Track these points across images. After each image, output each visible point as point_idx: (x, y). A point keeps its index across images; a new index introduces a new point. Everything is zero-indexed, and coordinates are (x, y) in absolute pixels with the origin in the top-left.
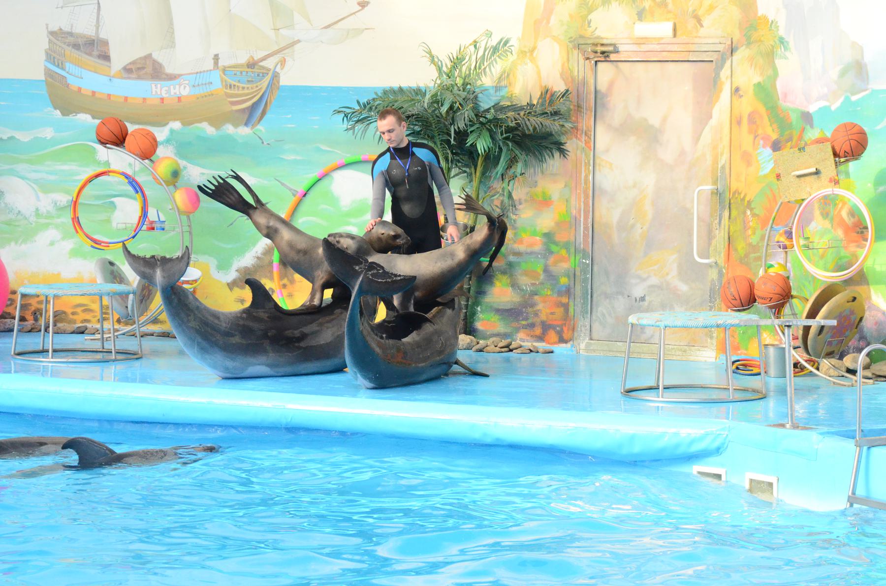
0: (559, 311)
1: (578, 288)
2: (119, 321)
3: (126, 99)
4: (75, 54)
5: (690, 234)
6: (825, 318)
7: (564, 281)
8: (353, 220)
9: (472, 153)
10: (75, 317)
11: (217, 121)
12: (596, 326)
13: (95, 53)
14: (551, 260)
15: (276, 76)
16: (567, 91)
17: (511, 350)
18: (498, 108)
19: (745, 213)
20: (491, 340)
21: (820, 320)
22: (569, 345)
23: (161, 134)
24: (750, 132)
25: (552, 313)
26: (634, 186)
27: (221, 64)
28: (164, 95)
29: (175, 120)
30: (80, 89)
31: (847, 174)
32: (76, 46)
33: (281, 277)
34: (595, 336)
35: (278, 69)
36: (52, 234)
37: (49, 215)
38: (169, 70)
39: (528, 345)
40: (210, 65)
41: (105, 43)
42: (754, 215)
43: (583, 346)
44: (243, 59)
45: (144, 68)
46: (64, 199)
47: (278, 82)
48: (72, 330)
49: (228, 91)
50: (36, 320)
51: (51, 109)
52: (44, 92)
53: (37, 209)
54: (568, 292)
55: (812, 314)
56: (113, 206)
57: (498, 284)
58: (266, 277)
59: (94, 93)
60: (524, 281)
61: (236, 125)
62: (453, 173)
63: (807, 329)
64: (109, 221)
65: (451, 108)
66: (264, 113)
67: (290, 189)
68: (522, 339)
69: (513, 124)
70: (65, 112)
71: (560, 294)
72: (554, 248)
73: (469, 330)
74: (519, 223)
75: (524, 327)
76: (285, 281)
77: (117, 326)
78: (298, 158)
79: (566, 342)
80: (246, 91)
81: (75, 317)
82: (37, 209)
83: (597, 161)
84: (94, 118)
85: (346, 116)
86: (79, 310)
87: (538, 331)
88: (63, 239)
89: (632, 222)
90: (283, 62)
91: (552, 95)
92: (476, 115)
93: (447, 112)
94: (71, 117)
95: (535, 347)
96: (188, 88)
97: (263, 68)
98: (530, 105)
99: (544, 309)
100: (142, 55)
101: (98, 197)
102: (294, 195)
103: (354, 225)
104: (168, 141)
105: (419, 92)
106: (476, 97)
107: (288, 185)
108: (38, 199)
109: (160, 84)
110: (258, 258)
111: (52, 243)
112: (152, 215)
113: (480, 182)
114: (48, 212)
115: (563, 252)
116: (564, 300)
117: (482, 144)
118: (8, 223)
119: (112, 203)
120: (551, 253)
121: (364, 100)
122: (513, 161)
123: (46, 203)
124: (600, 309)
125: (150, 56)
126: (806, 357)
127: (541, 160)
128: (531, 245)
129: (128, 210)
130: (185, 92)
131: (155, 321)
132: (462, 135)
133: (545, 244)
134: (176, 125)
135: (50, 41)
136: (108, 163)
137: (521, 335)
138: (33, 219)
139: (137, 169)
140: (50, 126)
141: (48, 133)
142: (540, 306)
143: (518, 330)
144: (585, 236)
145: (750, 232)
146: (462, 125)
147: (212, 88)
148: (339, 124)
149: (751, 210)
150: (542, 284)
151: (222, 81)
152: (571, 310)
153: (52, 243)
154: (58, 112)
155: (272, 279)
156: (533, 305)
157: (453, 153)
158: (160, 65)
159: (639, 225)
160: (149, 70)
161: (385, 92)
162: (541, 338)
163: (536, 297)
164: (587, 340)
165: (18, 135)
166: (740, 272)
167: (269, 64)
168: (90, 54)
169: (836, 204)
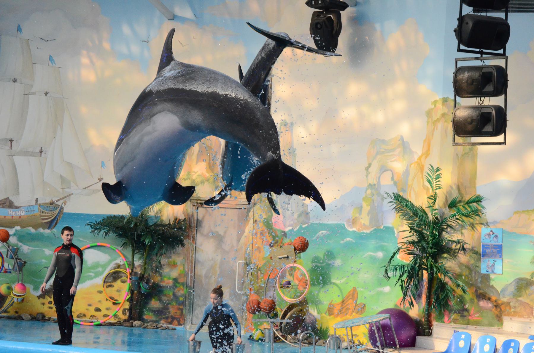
0: (179, 312)
1: (187, 303)
5: (235, 281)
6: (290, 319)
7: (181, 299)
8: (92, 271)
9: (144, 245)
11: (36, 227)
12: (194, 318)
14: (176, 290)
15: (62, 208)
16: (185, 219)
17: (158, 328)
18: (156, 225)
19: (258, 273)
20: (150, 323)
21: (286, 321)
22: (182, 326)
23: (11, 232)
24: (260, 238)
25: (176, 313)
26: (212, 259)
27: (38, 202)
28: (14, 215)
31: (300, 258)
34: (194, 322)
35: (63, 206)
38: (16, 204)
39: (165, 326)
40: (34, 203)
42: (261, 273)
43: (188, 327)
44: (48, 201)
49: (41, 214)
54: (183, 303)
55: (284, 317)
57: (153, 300)
60: (164, 299)
61: (44, 229)
62: (136, 252)
63: (281, 323)
65: (136, 225)
66: (56, 224)
68: (163, 323)
69: (161, 232)
71: (179, 304)
72: (178, 285)
73: (140, 318)
74: (163, 274)
75: (164, 318)
79: (181, 325)
83: (197, 249)
85: (91, 226)
87: (170, 320)
89: (210, 275)
91: (180, 220)
92: (147, 228)
93: (134, 226)
95: (168, 327)
96: (24, 212)
97: (57, 205)
98: (169, 224)
99: (173, 310)
100: (5, 197)
103: (93, 272)
104: (14, 235)
105: (123, 217)
106: (147, 220)
112: (6, 266)
113: (147, 256)
115: (181, 287)
116: (181, 307)
117: (147, 242)
120: (176, 287)
121: (98, 221)
122: (161, 248)
124: (196, 311)
125: (8, 198)
126: (282, 334)
127: (174, 248)
128: (168, 283)
131: (5, 311)
132: (139, 236)
133: (174, 283)
134: (18, 228)
137: (162, 322)
142: (171, 310)
143: (161, 319)
144: (191, 280)
145: (259, 281)
146: (139, 232)
147: (35, 213)
148: (88, 229)
149: (261, 271)
150: (172, 300)
152: (184, 311)
156: (168, 309)
157: (136, 244)
158: (13, 202)
159: (213, 276)
160: (8, 204)
161: (108, 217)
162: (171, 323)
163: (169, 306)
164: (190, 324)
166: (254, 297)
167: (59, 203)
169: (295, 270)
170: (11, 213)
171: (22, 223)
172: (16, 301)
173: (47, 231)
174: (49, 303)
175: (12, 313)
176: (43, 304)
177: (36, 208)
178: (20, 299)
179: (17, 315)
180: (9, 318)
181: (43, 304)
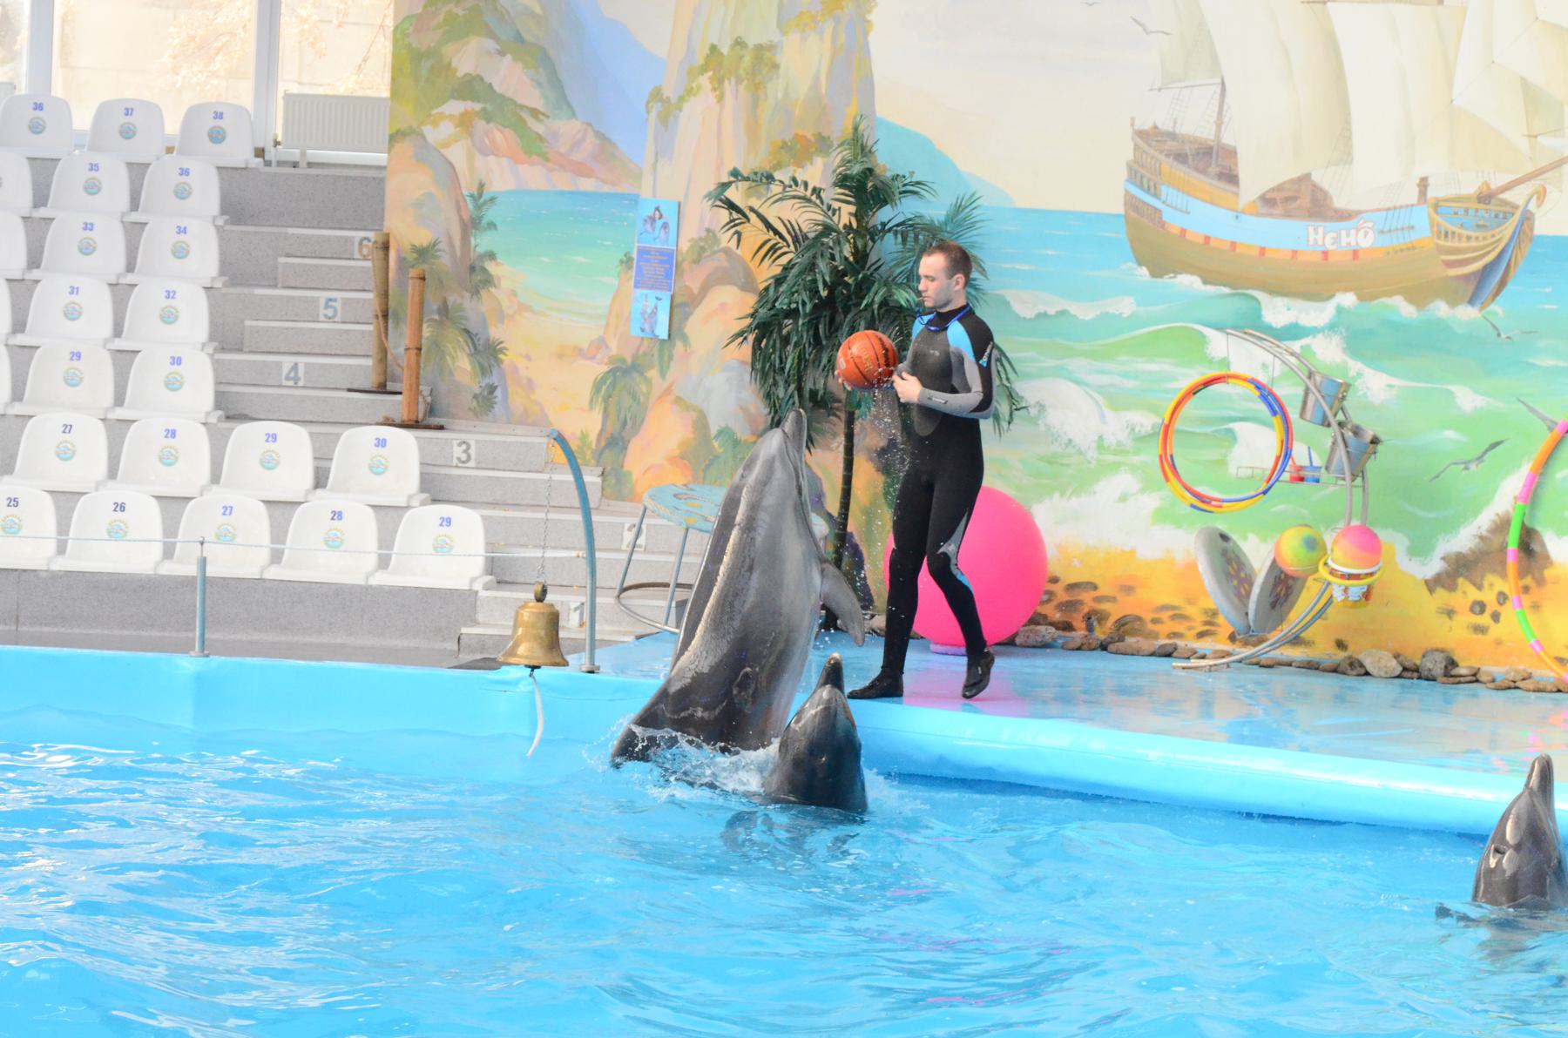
2: (1232, 638)
3: (1263, 250)
4: (1180, 170)
10: (1157, 628)
11: (1419, 295)
13: (1213, 169)
15: (1527, 218)
28: (1329, 246)
29: (1346, 290)
30: (1183, 231)
32: (1181, 157)
33: (1522, 573)
35: (1532, 207)
36: (1125, 481)
37: (1120, 450)
38: (1339, 202)
40: (1412, 195)
41: (1231, 153)
44: (1470, 187)
45: (1294, 198)
46: (1148, 421)
47: (1532, 229)
48: (1152, 649)
49: (1442, 242)
50: (1090, 629)
51: (1132, 264)
52: (1121, 234)
53: (1101, 438)
56: (1231, 436)
58: (1494, 571)
59: (1207, 239)
61: (1453, 304)
64: (1222, 463)
66: (1503, 283)
67: (1544, 419)
70: (1157, 272)
76: (1528, 580)
77: (1228, 647)
78: (1561, 364)
80: (1473, 244)
81: (1157, 628)
82: (1101, 438)
84: (1205, 282)
86: (1165, 615)
88: (1143, 491)
90: (1541, 195)
94: (1166, 279)
96: (1371, 236)
97: (1505, 203)
101: (1206, 421)
102: (1550, 429)
104: (1332, 327)
107: (1541, 411)
108: (1103, 417)
109: (1322, 226)
110: (1481, 538)
111: (1123, 498)
112: (1300, 454)
114: (1119, 443)
118: (1051, 460)
119: (1230, 431)
123: (1116, 427)
129: (1257, 445)
130: (1366, 241)
131: (1296, 641)
134: (1348, 299)
135: (1136, 148)
136: (1225, 362)
138: (1092, 454)
139: (1277, 374)
140: (1128, 293)
141: (1126, 306)
151: (1432, 227)
153: (1123, 498)
154: (1144, 271)
155: (1504, 575)
158: (1325, 194)
160: (1305, 201)
165: (1074, 309)
167: (1517, 196)
168: (1204, 172)
170: (1311, 237)
171: (1364, 275)
172: (1338, 596)
173: (1467, 314)
174: (1472, 610)
175: (1322, 650)
176: (1450, 613)
177: (1421, 221)
178: (1356, 589)
179: (1341, 655)
180: (1312, 666)
181: (1450, 613)
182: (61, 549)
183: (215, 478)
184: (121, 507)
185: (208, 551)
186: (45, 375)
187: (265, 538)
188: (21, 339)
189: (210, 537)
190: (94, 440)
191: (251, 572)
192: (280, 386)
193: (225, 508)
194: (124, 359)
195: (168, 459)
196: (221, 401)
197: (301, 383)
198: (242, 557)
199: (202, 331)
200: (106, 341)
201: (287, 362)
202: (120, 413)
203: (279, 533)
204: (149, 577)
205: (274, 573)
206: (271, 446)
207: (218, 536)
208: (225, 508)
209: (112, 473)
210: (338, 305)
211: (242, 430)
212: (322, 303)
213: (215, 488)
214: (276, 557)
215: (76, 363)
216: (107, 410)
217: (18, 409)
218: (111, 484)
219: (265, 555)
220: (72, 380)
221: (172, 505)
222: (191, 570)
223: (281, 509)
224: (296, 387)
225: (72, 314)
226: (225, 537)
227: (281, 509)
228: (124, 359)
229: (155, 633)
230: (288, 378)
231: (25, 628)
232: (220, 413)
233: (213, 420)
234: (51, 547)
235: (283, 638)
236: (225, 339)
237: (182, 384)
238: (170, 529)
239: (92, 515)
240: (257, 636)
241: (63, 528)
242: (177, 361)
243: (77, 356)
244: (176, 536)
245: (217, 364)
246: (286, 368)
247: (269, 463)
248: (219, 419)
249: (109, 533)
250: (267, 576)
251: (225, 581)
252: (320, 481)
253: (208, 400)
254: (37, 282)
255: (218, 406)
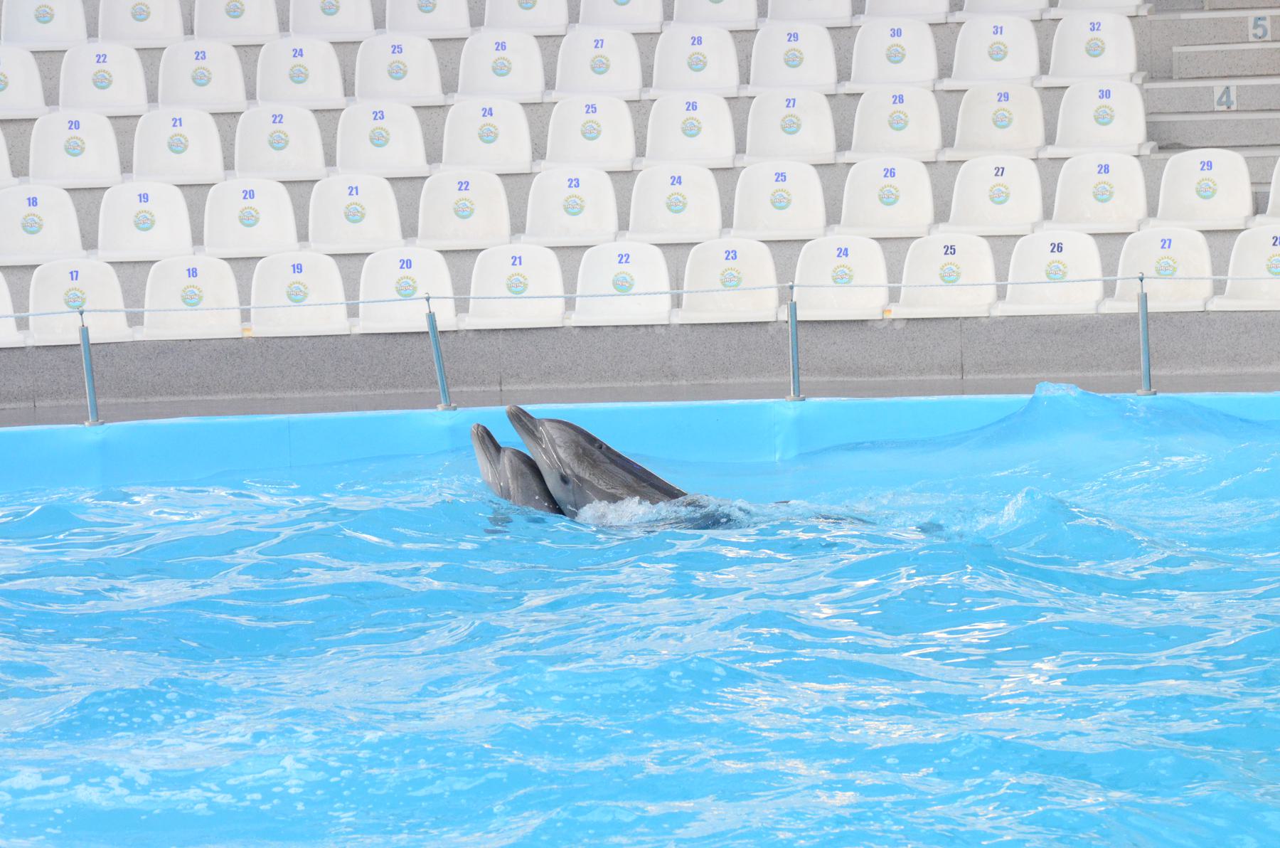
182: (1001, 294)
183: (1152, 211)
184: (1058, 248)
185: (1149, 286)
186: (974, 118)
187: (1207, 270)
188: (947, 84)
189: (1149, 272)
190: (1026, 180)
191: (1196, 306)
192: (1213, 112)
193: (1164, 241)
194: (1052, 96)
195: (1102, 195)
196: (1153, 131)
197: (1234, 107)
198: (1184, 290)
199: (1129, 62)
200: (1033, 79)
201: (1218, 86)
202: (1051, 152)
203: (1220, 264)
204: (1090, 317)
205: (1217, 304)
206: (1206, 173)
207: (1158, 271)
208: (1164, 241)
209: (1048, 213)
210: (1267, 23)
211: (1176, 160)
212: (1251, 24)
213: (1152, 221)
214: (1219, 288)
215: (1004, 104)
216: (1039, 149)
217: (949, 155)
218: (1047, 224)
219: (1207, 287)
220: (1001, 122)
221: (1110, 241)
222: (1132, 307)
223: (1219, 238)
224: (1229, 110)
225: (997, 54)
226: (1166, 271)
227: (1219, 238)
228: (1052, 96)
229: (1101, 374)
230: (1220, 103)
231: (970, 377)
232: (1153, 144)
233: (1147, 152)
234: (991, 292)
235: (1231, 370)
236: (1154, 67)
237: (1112, 117)
238: (1109, 267)
239: (1030, 258)
240: (1204, 370)
241: (1001, 273)
242: (1105, 94)
243: (1004, 96)
244: (1115, 273)
245: (1147, 95)
246: (1217, 95)
247: (1206, 192)
248: (1152, 151)
249: (1048, 275)
250: (1211, 307)
251: (1169, 316)
252: (1259, 206)
253: (1138, 130)
254: (960, 24)
255: (1150, 137)
